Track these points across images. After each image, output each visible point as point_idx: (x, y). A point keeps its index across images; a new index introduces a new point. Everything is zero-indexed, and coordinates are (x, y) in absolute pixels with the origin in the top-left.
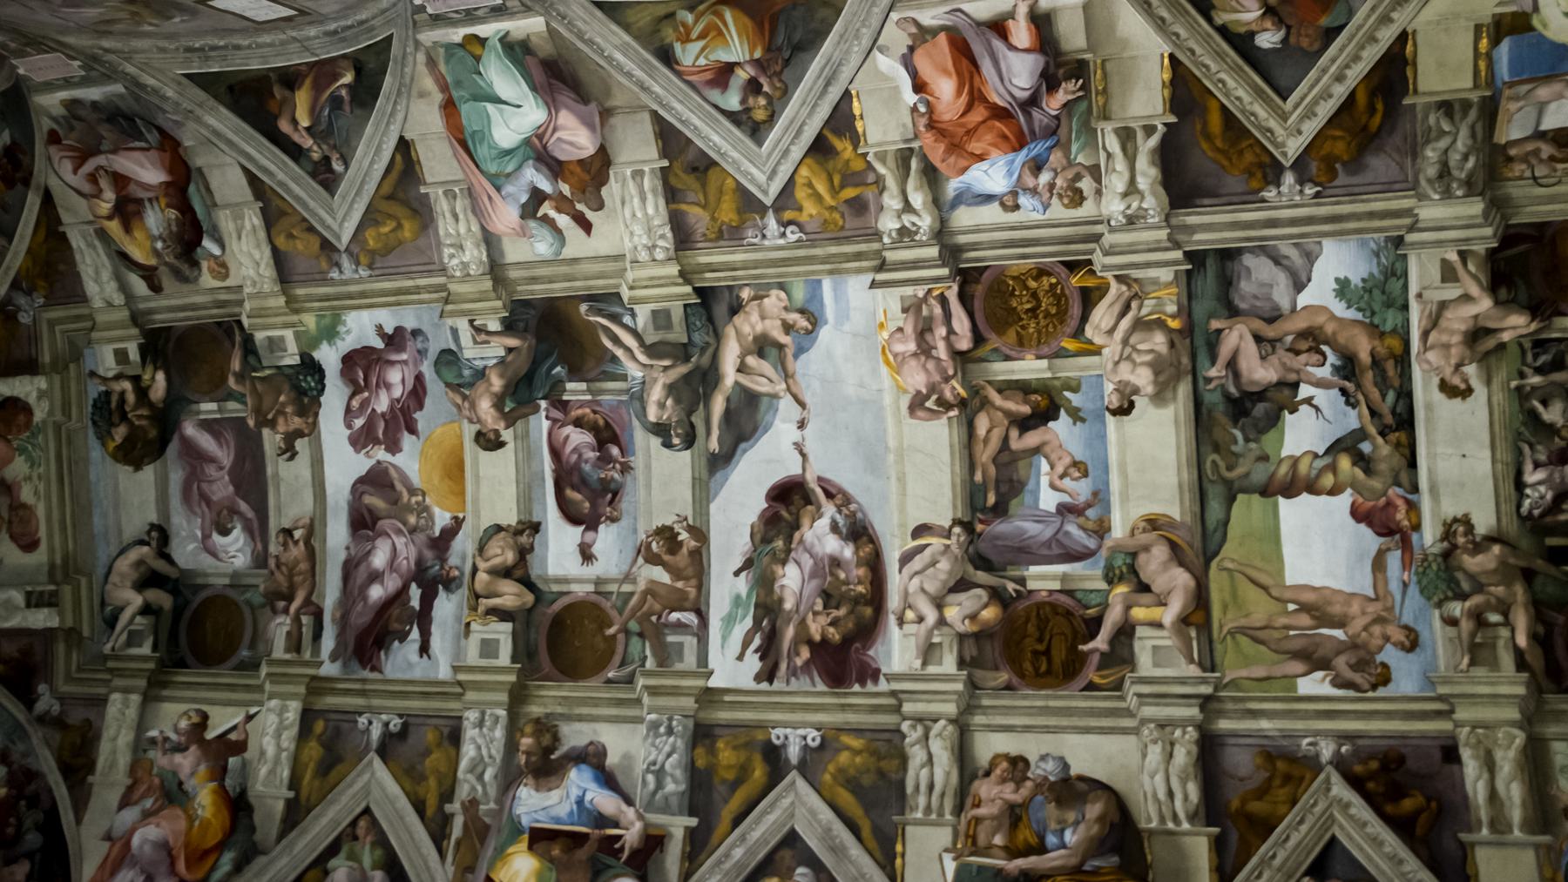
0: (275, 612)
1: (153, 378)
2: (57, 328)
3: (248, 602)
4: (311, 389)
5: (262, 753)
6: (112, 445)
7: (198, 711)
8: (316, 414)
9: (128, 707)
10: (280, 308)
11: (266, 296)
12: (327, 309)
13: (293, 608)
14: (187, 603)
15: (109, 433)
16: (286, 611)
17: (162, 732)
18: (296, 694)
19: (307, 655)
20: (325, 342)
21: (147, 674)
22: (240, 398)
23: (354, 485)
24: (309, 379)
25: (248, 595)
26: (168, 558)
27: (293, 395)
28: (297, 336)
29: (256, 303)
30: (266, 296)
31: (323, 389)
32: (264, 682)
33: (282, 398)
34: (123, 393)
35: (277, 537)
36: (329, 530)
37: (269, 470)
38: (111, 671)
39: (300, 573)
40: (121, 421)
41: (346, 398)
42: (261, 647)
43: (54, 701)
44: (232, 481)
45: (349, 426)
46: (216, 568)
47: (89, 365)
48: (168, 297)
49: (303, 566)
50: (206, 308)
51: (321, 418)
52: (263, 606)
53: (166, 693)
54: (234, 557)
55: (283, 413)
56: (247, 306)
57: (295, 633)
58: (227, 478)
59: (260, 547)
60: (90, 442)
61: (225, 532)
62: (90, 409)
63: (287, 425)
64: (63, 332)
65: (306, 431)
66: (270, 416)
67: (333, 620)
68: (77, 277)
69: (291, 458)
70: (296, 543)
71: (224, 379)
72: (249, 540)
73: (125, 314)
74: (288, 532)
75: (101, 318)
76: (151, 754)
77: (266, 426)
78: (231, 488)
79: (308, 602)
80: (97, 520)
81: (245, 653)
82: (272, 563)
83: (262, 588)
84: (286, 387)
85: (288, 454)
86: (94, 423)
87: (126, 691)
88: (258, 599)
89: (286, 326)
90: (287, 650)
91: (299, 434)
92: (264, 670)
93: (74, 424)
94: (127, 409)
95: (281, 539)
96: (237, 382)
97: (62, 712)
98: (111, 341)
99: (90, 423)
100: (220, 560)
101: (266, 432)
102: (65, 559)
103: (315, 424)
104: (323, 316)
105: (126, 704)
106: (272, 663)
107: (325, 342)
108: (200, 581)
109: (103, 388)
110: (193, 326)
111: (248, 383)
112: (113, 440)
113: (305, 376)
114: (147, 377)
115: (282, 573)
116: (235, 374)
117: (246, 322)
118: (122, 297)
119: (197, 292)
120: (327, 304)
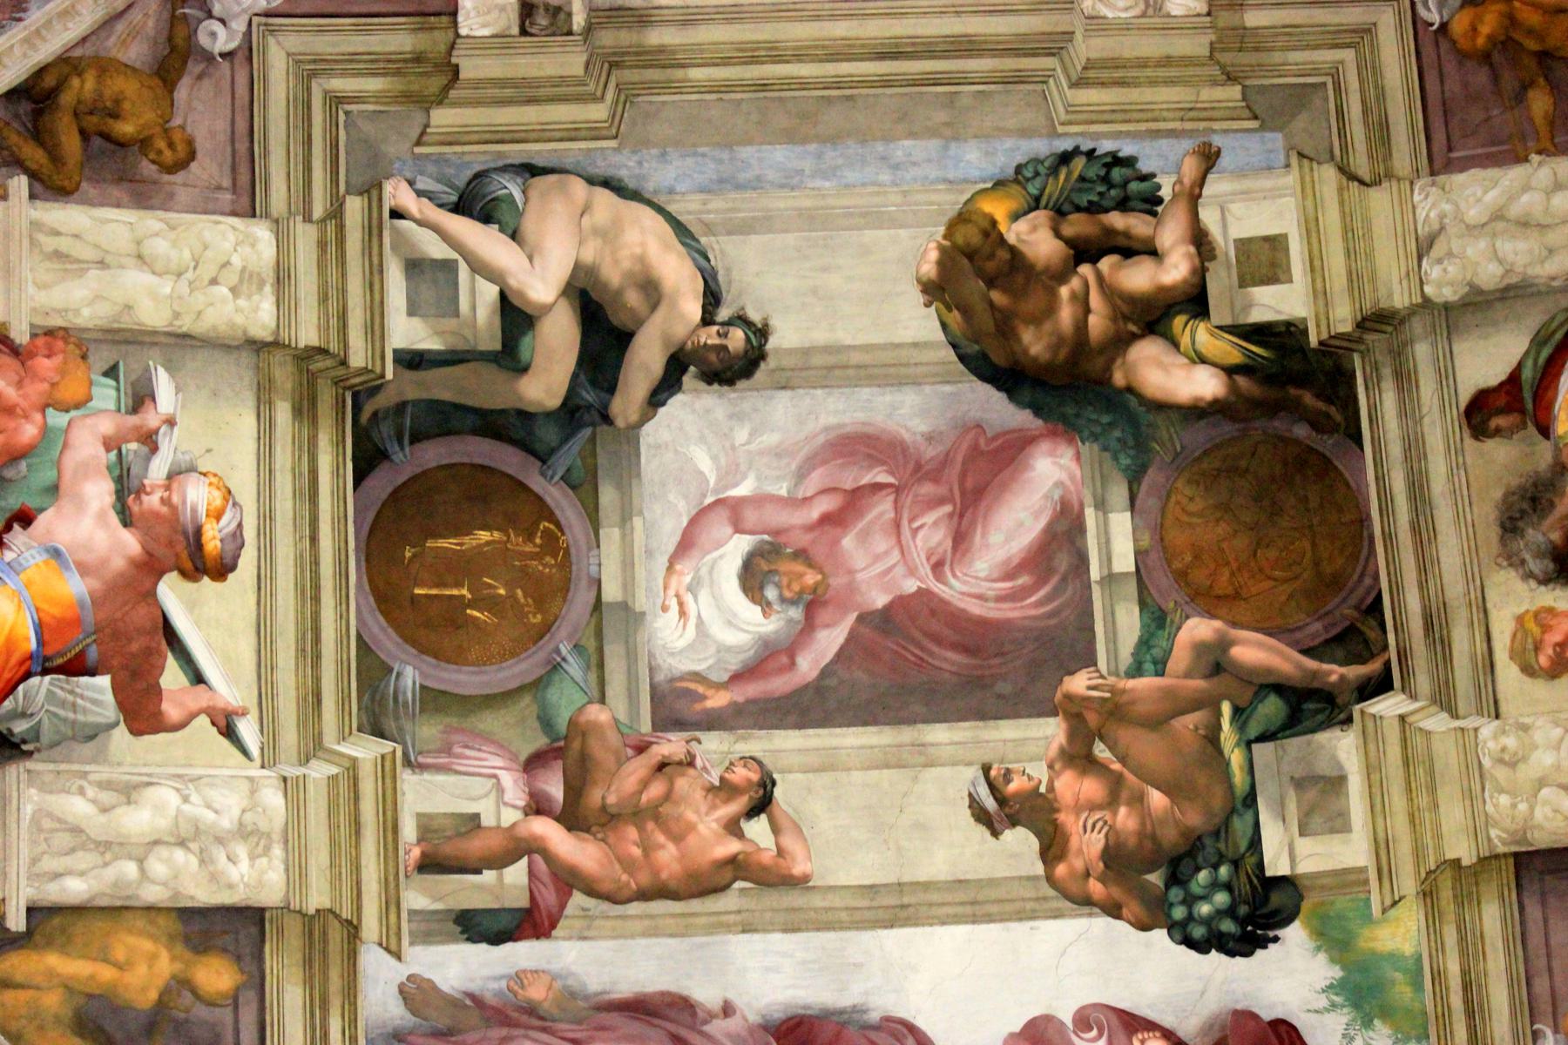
0: (534, 763)
1: (1202, 360)
2: (1348, 55)
3: (555, 667)
4: (1190, 901)
5: (129, 792)
6: (997, 208)
7: (237, 536)
8: (1114, 910)
9: (234, 290)
10: (1438, 836)
11: (1472, 798)
12: (1441, 996)
13: (547, 829)
14: (543, 458)
15: (1035, 204)
16: (537, 806)
17: (171, 422)
18: (303, 874)
19: (418, 897)
20: (1336, 973)
21: (334, 347)
22: (1148, 656)
23: (911, 1029)
24: (1221, 898)
25: (574, 667)
26: (668, 384)
27: (1170, 837)
28: (1349, 880)
29: (1447, 754)
30: (1472, 798)
31: (1189, 942)
32: (333, 757)
33: (1157, 799)
34: (1153, 253)
35: (747, 760)
36: (778, 940)
37: (939, 734)
38: (336, 213)
39: (647, 848)
40: (1069, 242)
41: (1167, 1021)
42: (428, 731)
43: (239, 26)
44: (901, 603)
45: (1084, 1020)
46: (649, 553)
47: (1237, 147)
48: (1454, 451)
49: (668, 857)
50: (1423, 570)
51: (1101, 924)
52: (546, 723)
53: (283, 413)
54: (683, 613)
55: (1112, 802)
56: (1438, 722)
57: (475, 846)
58: (911, 586)
59: (718, 700)
60: (1009, 143)
61: (753, 578)
62: (1106, 146)
63: (1078, 808)
64: (1335, 73)
65: (1061, 870)
66: (1101, 751)
67: (519, 977)
68: (1505, 150)
69: (981, 815)
70: (733, 828)
71: (1208, 601)
72: (734, 663)
73: (1400, 299)
74: (762, 804)
75: (1380, 201)
76: (105, 395)
77: (1072, 735)
78: (880, 600)
79: (568, 880)
80: (780, 154)
81: (410, 676)
82: (672, 745)
83: (598, 714)
84: (1194, 818)
85: (990, 804)
86: (1065, 158)
87: (282, 277)
88: (565, 700)
89: (1382, 847)
90: (426, 826)
91: (1053, 847)
92: (366, 750)
93: (1062, 95)
94: (1105, 264)
95: (741, 774)
96: (1200, 649)
97: (209, 58)
98: (1311, 228)
99: (1066, 145)
100: (670, 568)
101: (1051, 731)
102: (661, 58)
103: (1085, 902)
104: (1418, 985)
105: (246, 282)
106: (387, 774)
107: (1336, 973)
108: (608, 496)
109: (1166, 192)
110: (1363, 520)
111: (1199, 684)
112: (1016, 217)
113: (1228, 887)
114: (1203, 336)
115: (645, 784)
116: (1223, 644)
117: (1387, 706)
118: (1449, 294)
119: (1472, 551)
120: (1456, 1001)
